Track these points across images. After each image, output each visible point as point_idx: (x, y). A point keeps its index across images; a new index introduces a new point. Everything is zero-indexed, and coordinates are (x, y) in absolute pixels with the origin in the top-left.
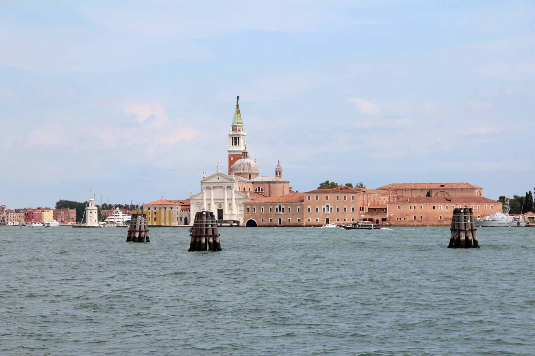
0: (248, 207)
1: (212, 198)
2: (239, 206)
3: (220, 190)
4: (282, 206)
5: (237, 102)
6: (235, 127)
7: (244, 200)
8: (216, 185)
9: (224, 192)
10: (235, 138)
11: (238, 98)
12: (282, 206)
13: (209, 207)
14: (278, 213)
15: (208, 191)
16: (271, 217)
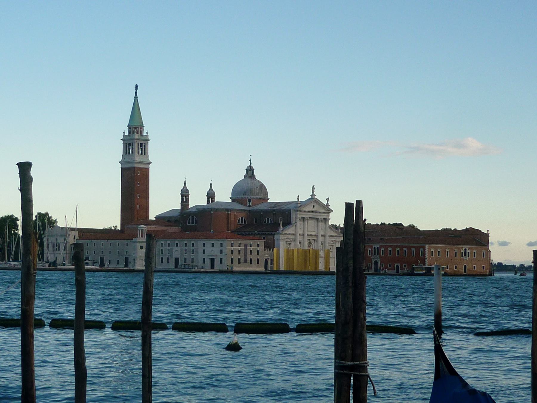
0: (432, 250)
1: (306, 233)
2: (331, 245)
3: (312, 223)
4: (467, 250)
5: (136, 92)
6: (140, 128)
7: (335, 238)
8: (312, 215)
9: (317, 226)
10: (141, 144)
11: (137, 87)
12: (467, 249)
13: (300, 245)
14: (464, 258)
15: (302, 223)
16: (457, 264)
